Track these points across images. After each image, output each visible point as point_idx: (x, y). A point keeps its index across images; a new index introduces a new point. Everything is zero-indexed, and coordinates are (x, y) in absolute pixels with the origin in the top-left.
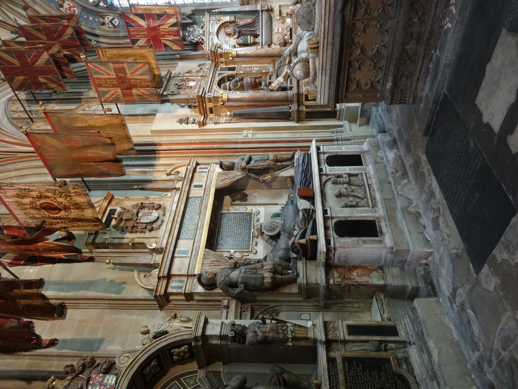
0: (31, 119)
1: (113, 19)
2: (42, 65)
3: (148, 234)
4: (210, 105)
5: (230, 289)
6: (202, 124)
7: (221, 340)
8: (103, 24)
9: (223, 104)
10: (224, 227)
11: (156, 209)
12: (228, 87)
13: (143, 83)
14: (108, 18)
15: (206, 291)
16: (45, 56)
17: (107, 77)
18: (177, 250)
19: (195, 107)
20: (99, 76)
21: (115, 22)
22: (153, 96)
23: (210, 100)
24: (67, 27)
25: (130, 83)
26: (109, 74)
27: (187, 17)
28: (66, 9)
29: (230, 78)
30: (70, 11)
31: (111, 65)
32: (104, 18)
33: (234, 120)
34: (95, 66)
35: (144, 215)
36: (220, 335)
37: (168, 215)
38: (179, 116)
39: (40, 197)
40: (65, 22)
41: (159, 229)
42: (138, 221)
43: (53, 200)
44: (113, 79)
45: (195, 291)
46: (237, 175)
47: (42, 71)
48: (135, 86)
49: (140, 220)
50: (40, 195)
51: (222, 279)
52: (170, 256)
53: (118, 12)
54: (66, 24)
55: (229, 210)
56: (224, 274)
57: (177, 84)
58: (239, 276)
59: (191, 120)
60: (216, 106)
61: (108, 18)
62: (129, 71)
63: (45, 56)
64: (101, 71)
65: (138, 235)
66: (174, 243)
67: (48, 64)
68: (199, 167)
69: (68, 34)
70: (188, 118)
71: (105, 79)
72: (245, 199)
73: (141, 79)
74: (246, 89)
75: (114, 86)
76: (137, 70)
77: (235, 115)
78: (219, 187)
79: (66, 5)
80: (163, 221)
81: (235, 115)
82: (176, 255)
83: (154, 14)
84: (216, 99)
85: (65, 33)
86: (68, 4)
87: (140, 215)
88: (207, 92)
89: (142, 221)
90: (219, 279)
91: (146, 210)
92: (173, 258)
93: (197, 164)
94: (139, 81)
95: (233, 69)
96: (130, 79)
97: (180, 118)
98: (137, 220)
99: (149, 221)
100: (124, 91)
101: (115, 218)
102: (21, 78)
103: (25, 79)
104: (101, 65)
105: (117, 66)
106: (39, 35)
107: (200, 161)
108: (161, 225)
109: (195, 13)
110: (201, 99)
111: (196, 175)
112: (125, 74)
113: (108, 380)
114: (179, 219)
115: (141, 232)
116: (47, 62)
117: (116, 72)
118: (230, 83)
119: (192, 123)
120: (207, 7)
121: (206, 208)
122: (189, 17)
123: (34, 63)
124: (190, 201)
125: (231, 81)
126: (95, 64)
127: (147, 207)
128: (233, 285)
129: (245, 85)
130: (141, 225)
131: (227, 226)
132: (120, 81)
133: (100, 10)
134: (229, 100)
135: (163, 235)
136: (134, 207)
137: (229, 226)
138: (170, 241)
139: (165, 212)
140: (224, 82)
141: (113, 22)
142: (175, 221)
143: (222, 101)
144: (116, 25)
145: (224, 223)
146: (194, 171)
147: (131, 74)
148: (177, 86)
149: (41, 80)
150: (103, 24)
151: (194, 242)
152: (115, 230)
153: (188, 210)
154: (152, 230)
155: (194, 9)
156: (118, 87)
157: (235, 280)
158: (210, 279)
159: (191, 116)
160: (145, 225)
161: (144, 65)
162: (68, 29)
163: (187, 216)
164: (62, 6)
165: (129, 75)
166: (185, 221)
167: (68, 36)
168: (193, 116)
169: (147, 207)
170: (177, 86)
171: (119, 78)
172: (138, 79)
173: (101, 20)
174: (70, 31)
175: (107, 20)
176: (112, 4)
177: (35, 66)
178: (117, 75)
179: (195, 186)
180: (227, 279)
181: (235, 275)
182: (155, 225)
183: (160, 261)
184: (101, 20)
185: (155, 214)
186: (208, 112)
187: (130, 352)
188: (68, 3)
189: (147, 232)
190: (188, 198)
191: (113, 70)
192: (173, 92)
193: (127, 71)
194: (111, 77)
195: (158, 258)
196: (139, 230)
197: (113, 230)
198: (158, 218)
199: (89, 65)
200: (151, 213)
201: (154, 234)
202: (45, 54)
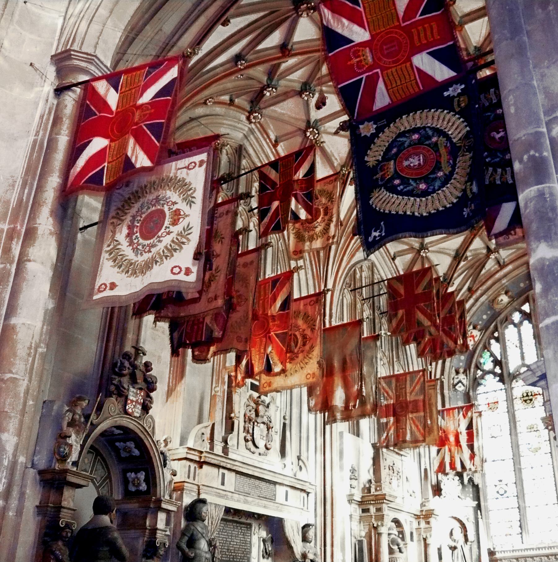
0: (355, 290)
1: (463, 385)
2: (416, 317)
3: (242, 435)
4: (373, 510)
5: (186, 538)
6: (351, 498)
7: (150, 530)
8: (457, 372)
9: (374, 527)
10: (237, 528)
11: (266, 446)
12: (391, 532)
13: (401, 431)
14: (464, 379)
15: (183, 507)
16: (427, 323)
17: (408, 390)
18: (226, 472)
19: (369, 490)
20: (408, 382)
21: (460, 387)
22: (386, 441)
23: (379, 510)
24: (456, 343)
25: (402, 415)
26: (411, 393)
27: (470, 478)
28: (471, 333)
29: (401, 533)
30: (470, 337)
31: (421, 397)
32: (463, 373)
33: (354, 540)
34: (420, 379)
35: (262, 431)
36: (157, 529)
37: (261, 458)
38: (358, 468)
39: (304, 337)
40: (460, 342)
41: (247, 449)
42: (256, 423)
43: (301, 349)
44: (406, 397)
45: (184, 495)
46: (298, 547)
47: (410, 315)
48: (397, 421)
49: (257, 426)
50: (306, 338)
51: (199, 529)
52: (222, 464)
53: (471, 391)
54: (459, 343)
55: (254, 534)
56: (204, 531)
57: (394, 464)
58: (202, 551)
59: (354, 483)
60: (372, 517)
61: (464, 379)
62: (415, 417)
63: (427, 323)
64: (414, 385)
65: (242, 424)
66: (234, 468)
67: (418, 324)
68: (305, 495)
69: (447, 341)
70: (356, 479)
71: (405, 387)
72: (266, 556)
73: (406, 429)
74: (391, 556)
75: (397, 397)
76: (417, 427)
77: (360, 542)
78: (285, 523)
79: (476, 333)
80: (253, 453)
81: (360, 542)
82: (222, 470)
83: (473, 441)
84: (381, 518)
85: (448, 339)
86: (477, 336)
87: (262, 425)
88: (389, 505)
89: (256, 428)
90: (199, 526)
91: (265, 432)
92: (218, 467)
93: (308, 493)
94: (404, 427)
95: (412, 539)
96: (406, 416)
97: (356, 469)
98: (258, 423)
99: (255, 437)
100: (392, 407)
101: (259, 397)
102: (402, 291)
103: (401, 295)
104: (421, 387)
105: (421, 404)
106: (446, 310)
107: (312, 496)
108: (250, 451)
109: (476, 488)
110: (380, 499)
111: (298, 492)
112: (412, 412)
113: (138, 408)
114: (256, 474)
115: (244, 428)
116: (419, 324)
117: (413, 401)
118: (396, 535)
119: (351, 485)
120: (482, 504)
121: (265, 507)
122: (471, 480)
123: (418, 308)
124: (272, 486)
125: (398, 536)
126: (422, 379)
127: (268, 433)
128: (192, 542)
129: (393, 556)
130: (252, 427)
131: (238, 532)
132: (404, 405)
133: (472, 370)
134: (380, 534)
135: (241, 454)
136: (269, 418)
137: (238, 534)
138: (236, 463)
139: (263, 455)
140: (397, 527)
141: (460, 384)
142: (255, 469)
143: (378, 525)
144: (457, 387)
145: (241, 527)
146: (302, 490)
147: (412, 418)
148: (392, 465)
149: (401, 312)
150: (457, 372)
151: (232, 492)
152: (248, 397)
153: (264, 483)
154: (246, 440)
155: (480, 486)
156: (396, 401)
157: (197, 546)
158: (200, 513)
159: (359, 483)
160: (251, 431)
161: (422, 434)
162: (453, 343)
163: (257, 482)
164: (474, 328)
165: (411, 416)
166: (252, 480)
167: (445, 341)
168: (358, 486)
169: (268, 433)
170: (392, 465)
171: (407, 403)
172: (406, 426)
173: (461, 370)
174: (451, 344)
175: (462, 377)
176: (479, 384)
177: (416, 309)
178: (410, 402)
179: (287, 492)
180: (200, 535)
181: (203, 545)
182: (250, 443)
183: (215, 452)
184: (461, 370)
185: (261, 443)
186: (365, 507)
187: (153, 428)
188: (478, 336)
189: (245, 434)
190: (275, 483)
191: (416, 398)
192: (386, 460)
193: (415, 415)
194: (408, 394)
195: (218, 449)
196: (247, 426)
197: (248, 394)
198: (257, 447)
199: (421, 373)
200: (263, 439)
201: (242, 442)
202: (429, 323)
